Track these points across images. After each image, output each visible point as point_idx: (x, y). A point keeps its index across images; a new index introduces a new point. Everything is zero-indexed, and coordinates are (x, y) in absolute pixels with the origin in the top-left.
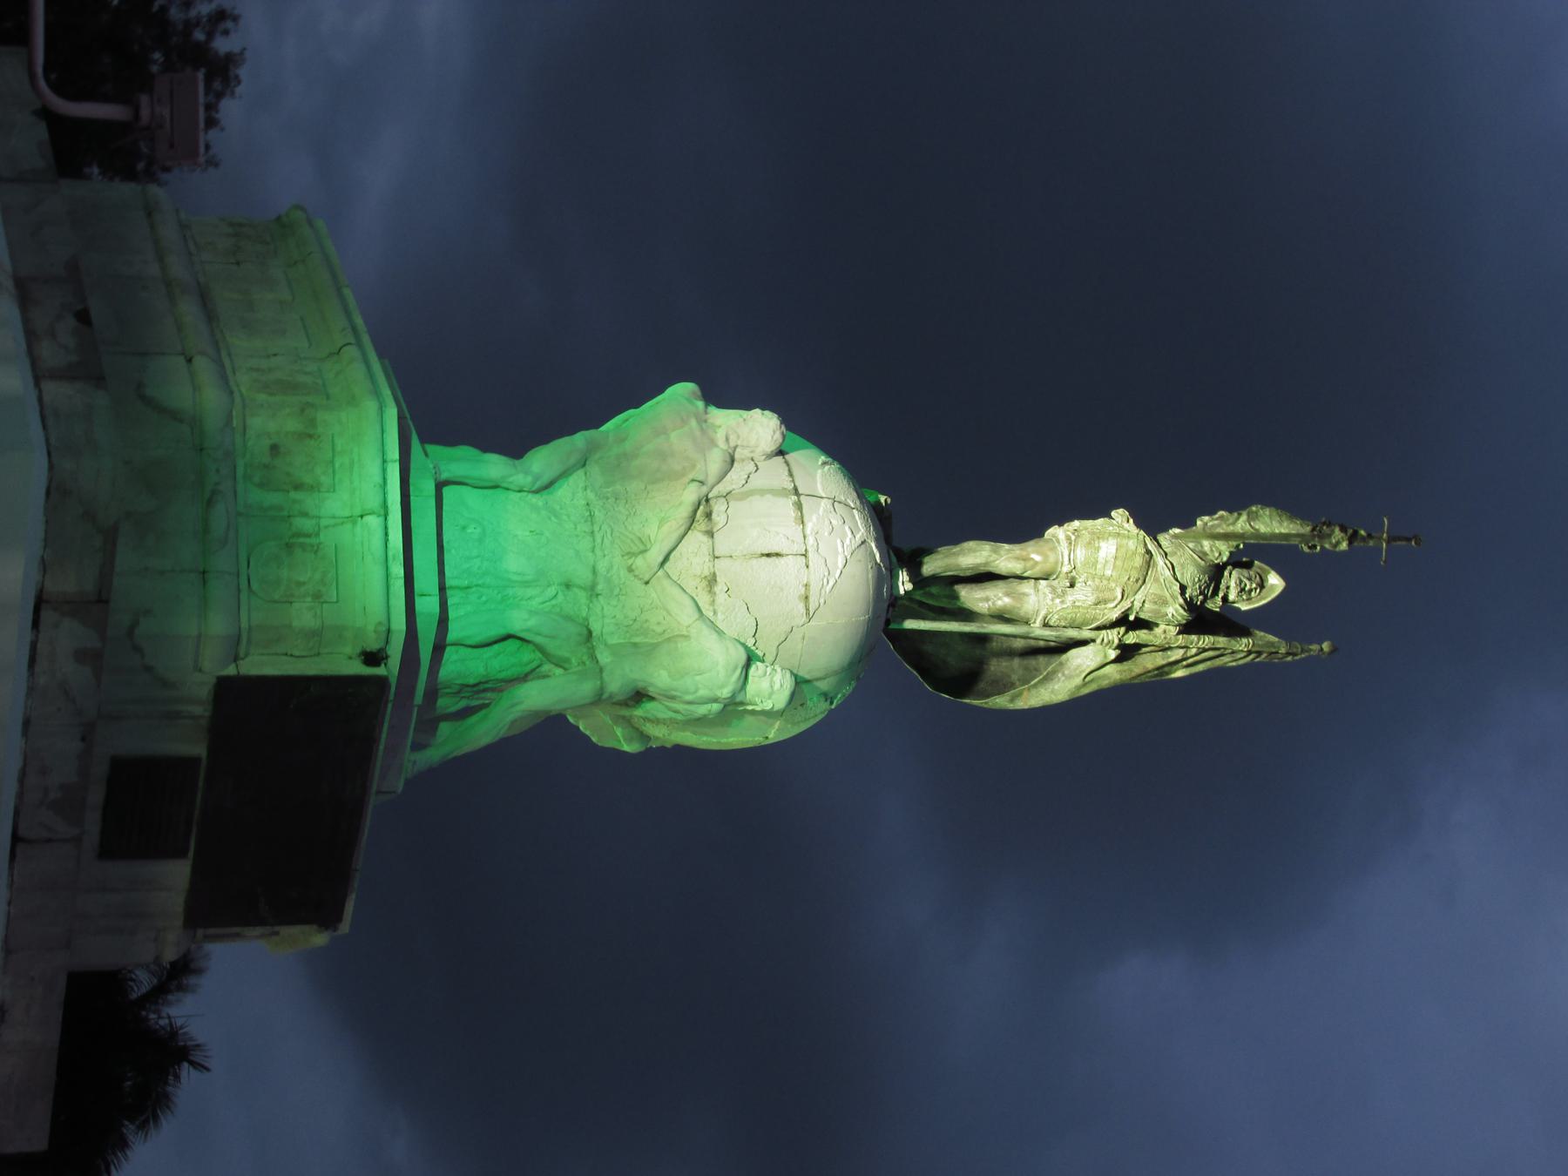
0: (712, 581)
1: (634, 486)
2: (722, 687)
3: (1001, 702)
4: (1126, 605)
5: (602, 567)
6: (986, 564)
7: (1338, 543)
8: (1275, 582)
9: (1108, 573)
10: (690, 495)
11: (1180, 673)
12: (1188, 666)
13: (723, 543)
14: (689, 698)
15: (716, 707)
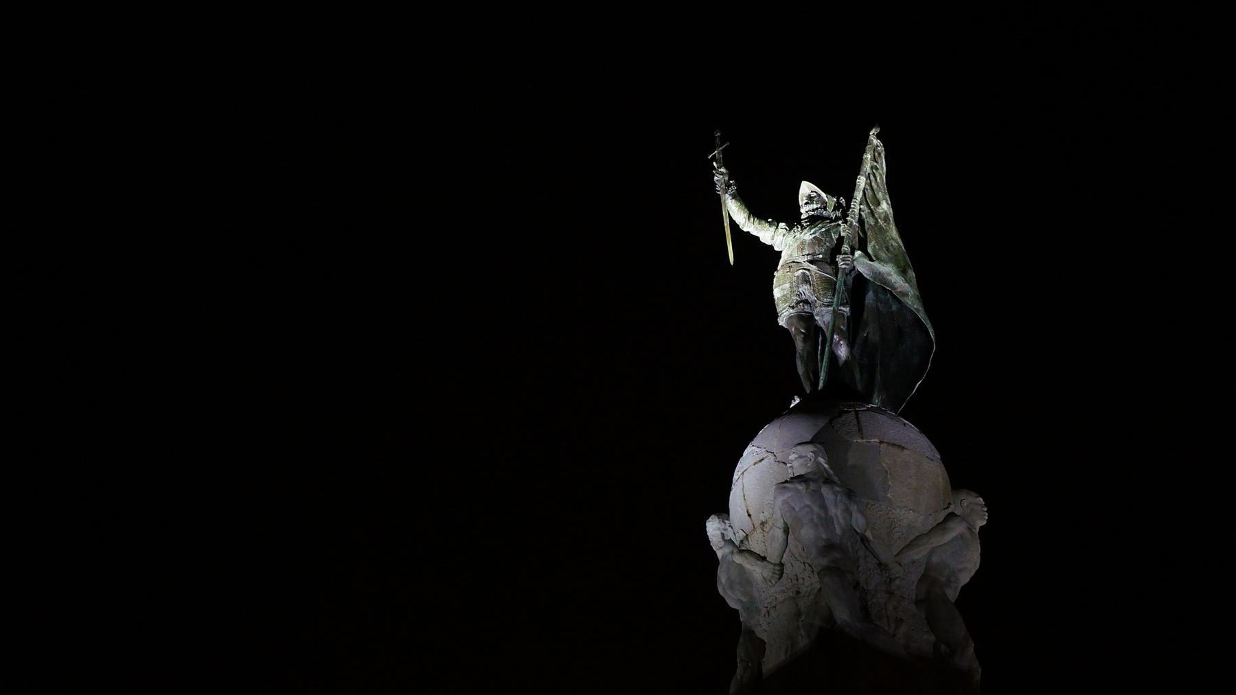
0: (763, 524)
1: (756, 594)
2: (797, 491)
3: (912, 301)
4: (807, 265)
5: (781, 597)
6: (802, 357)
7: (722, 174)
8: (806, 188)
9: (788, 285)
10: (738, 559)
11: (885, 206)
12: (879, 204)
13: (748, 529)
14: (816, 509)
15: (825, 491)
